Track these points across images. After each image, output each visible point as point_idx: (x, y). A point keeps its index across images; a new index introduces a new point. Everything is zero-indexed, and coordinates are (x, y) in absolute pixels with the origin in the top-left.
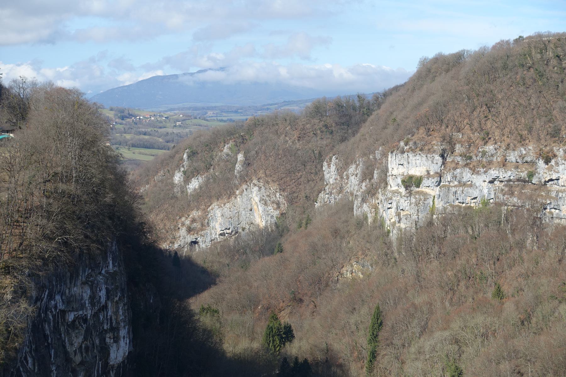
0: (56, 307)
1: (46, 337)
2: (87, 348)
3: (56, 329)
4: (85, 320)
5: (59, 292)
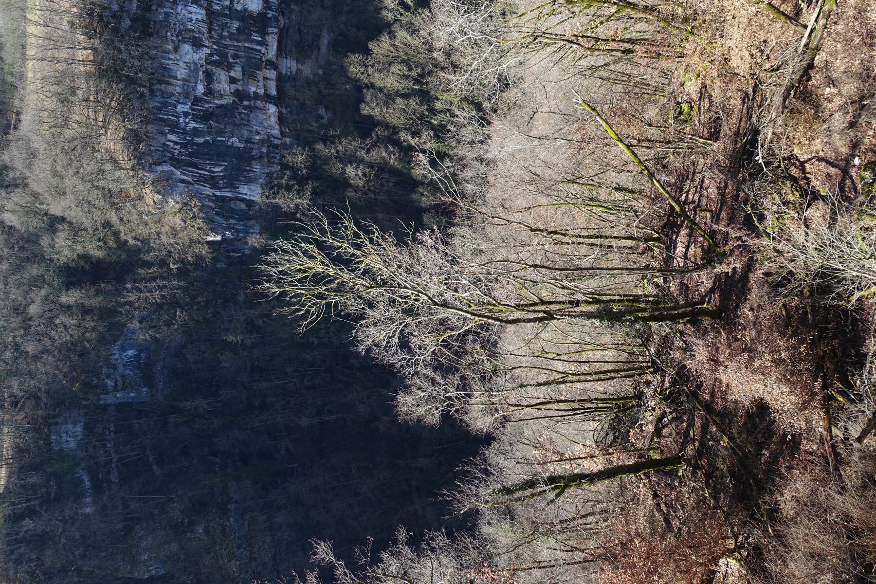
0: (186, 114)
1: (206, 142)
2: (235, 56)
3: (205, 117)
4: (211, 55)
5: (175, 106)
